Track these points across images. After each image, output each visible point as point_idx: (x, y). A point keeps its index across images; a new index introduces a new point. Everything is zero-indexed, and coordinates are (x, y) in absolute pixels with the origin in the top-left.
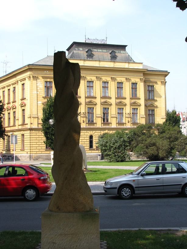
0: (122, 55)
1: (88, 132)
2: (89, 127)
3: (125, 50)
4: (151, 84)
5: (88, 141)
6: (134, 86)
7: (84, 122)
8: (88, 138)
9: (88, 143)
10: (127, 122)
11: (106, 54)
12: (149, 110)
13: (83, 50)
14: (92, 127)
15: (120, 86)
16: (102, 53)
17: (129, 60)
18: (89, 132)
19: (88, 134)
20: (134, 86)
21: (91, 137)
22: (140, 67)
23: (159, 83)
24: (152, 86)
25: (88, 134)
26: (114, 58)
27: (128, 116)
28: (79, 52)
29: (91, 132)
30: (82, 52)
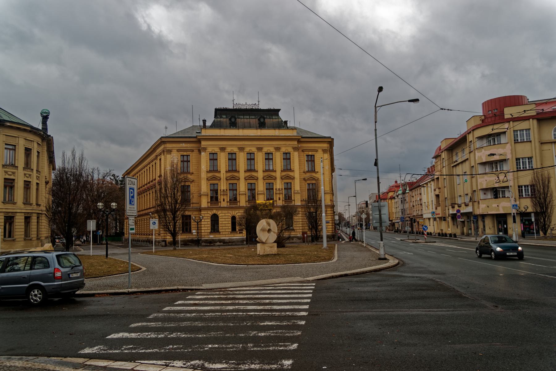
0: (275, 120)
1: (229, 212)
2: (231, 206)
3: (278, 115)
4: (310, 153)
5: (230, 222)
6: (287, 158)
7: (224, 201)
8: (230, 220)
9: (230, 225)
10: (278, 199)
11: (254, 121)
12: (309, 184)
13: (226, 118)
14: (234, 206)
15: (269, 157)
16: (248, 120)
17: (283, 125)
18: (231, 212)
19: (229, 214)
20: (287, 158)
21: (233, 218)
22: (294, 133)
23: (320, 151)
24: (311, 155)
25: (229, 214)
26: (262, 125)
27: (278, 192)
28: (222, 119)
29: (233, 212)
30: (225, 120)
